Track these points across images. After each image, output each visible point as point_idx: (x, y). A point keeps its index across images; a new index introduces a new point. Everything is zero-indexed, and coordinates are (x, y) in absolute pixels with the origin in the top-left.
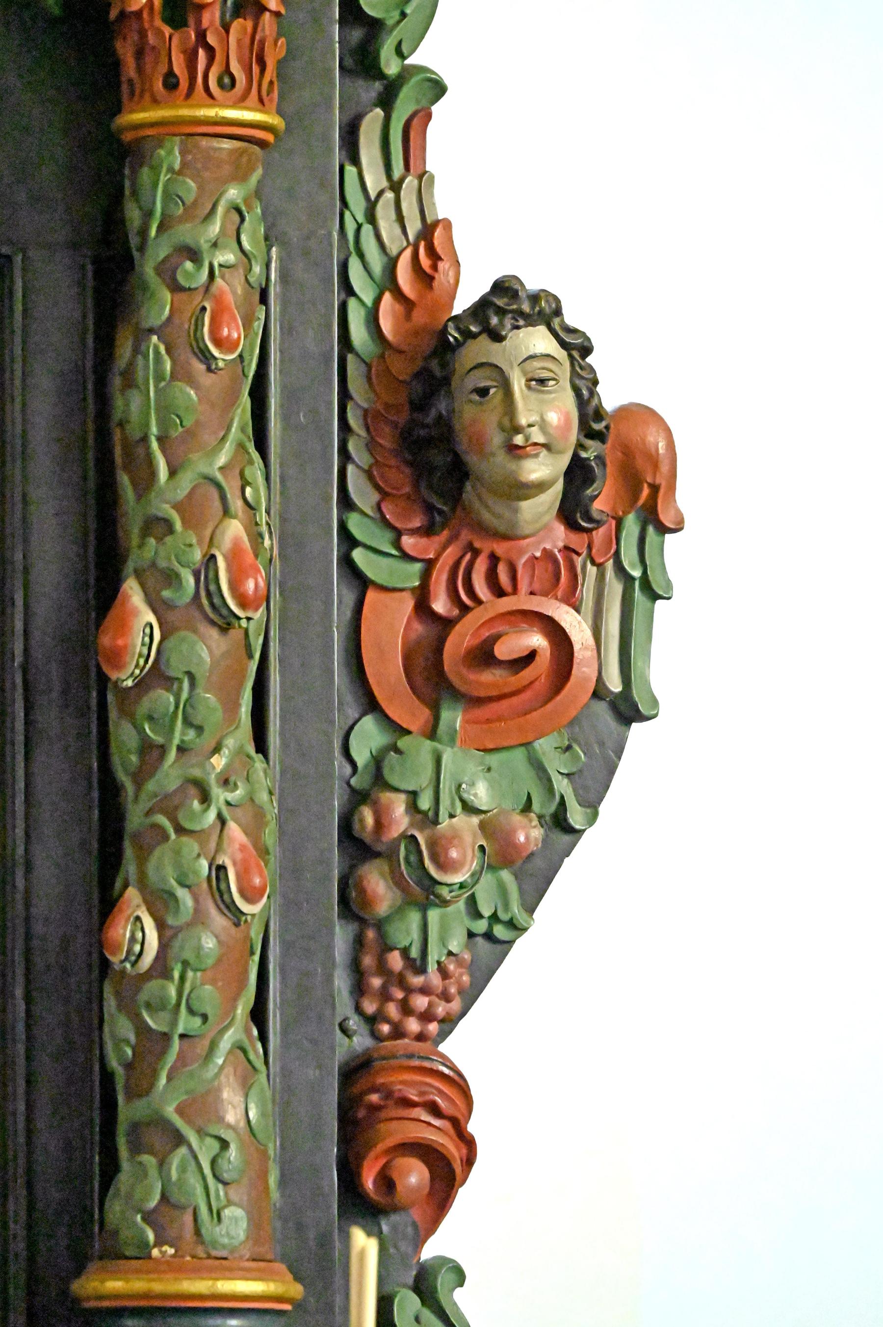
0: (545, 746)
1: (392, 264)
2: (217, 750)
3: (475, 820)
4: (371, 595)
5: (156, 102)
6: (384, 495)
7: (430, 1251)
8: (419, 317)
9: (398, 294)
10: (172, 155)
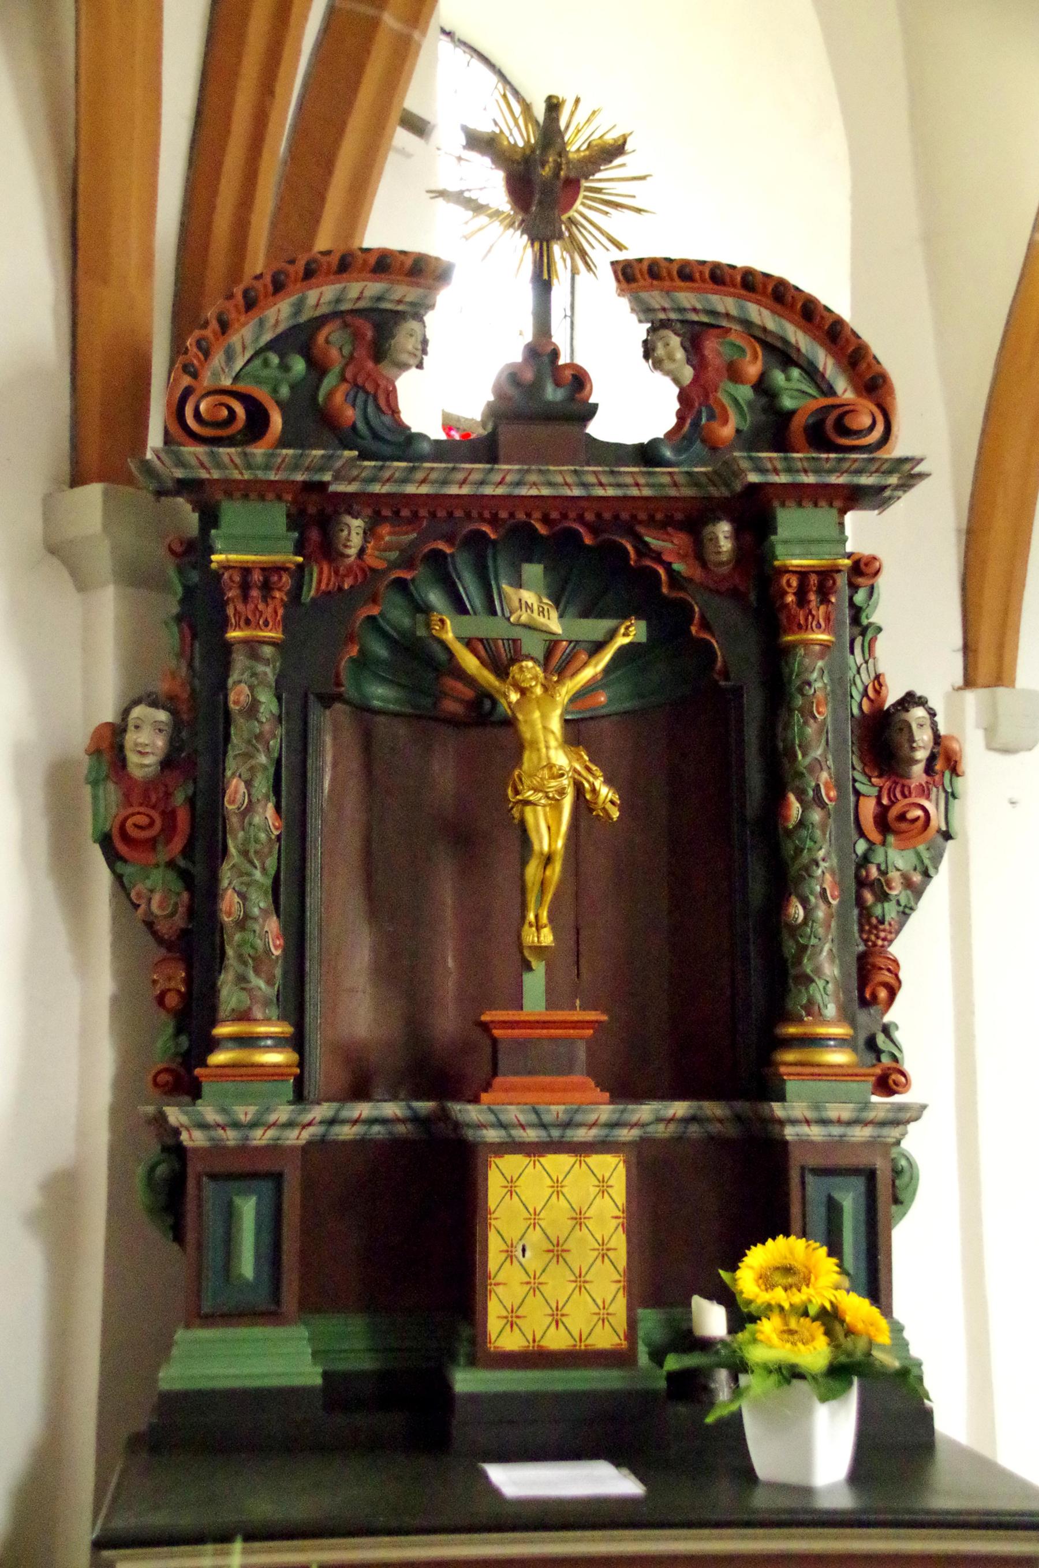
0: (921, 848)
1: (866, 688)
2: (821, 848)
3: (898, 873)
4: (862, 798)
5: (794, 633)
6: (865, 765)
7: (887, 1019)
8: (876, 705)
9: (869, 698)
10: (802, 651)
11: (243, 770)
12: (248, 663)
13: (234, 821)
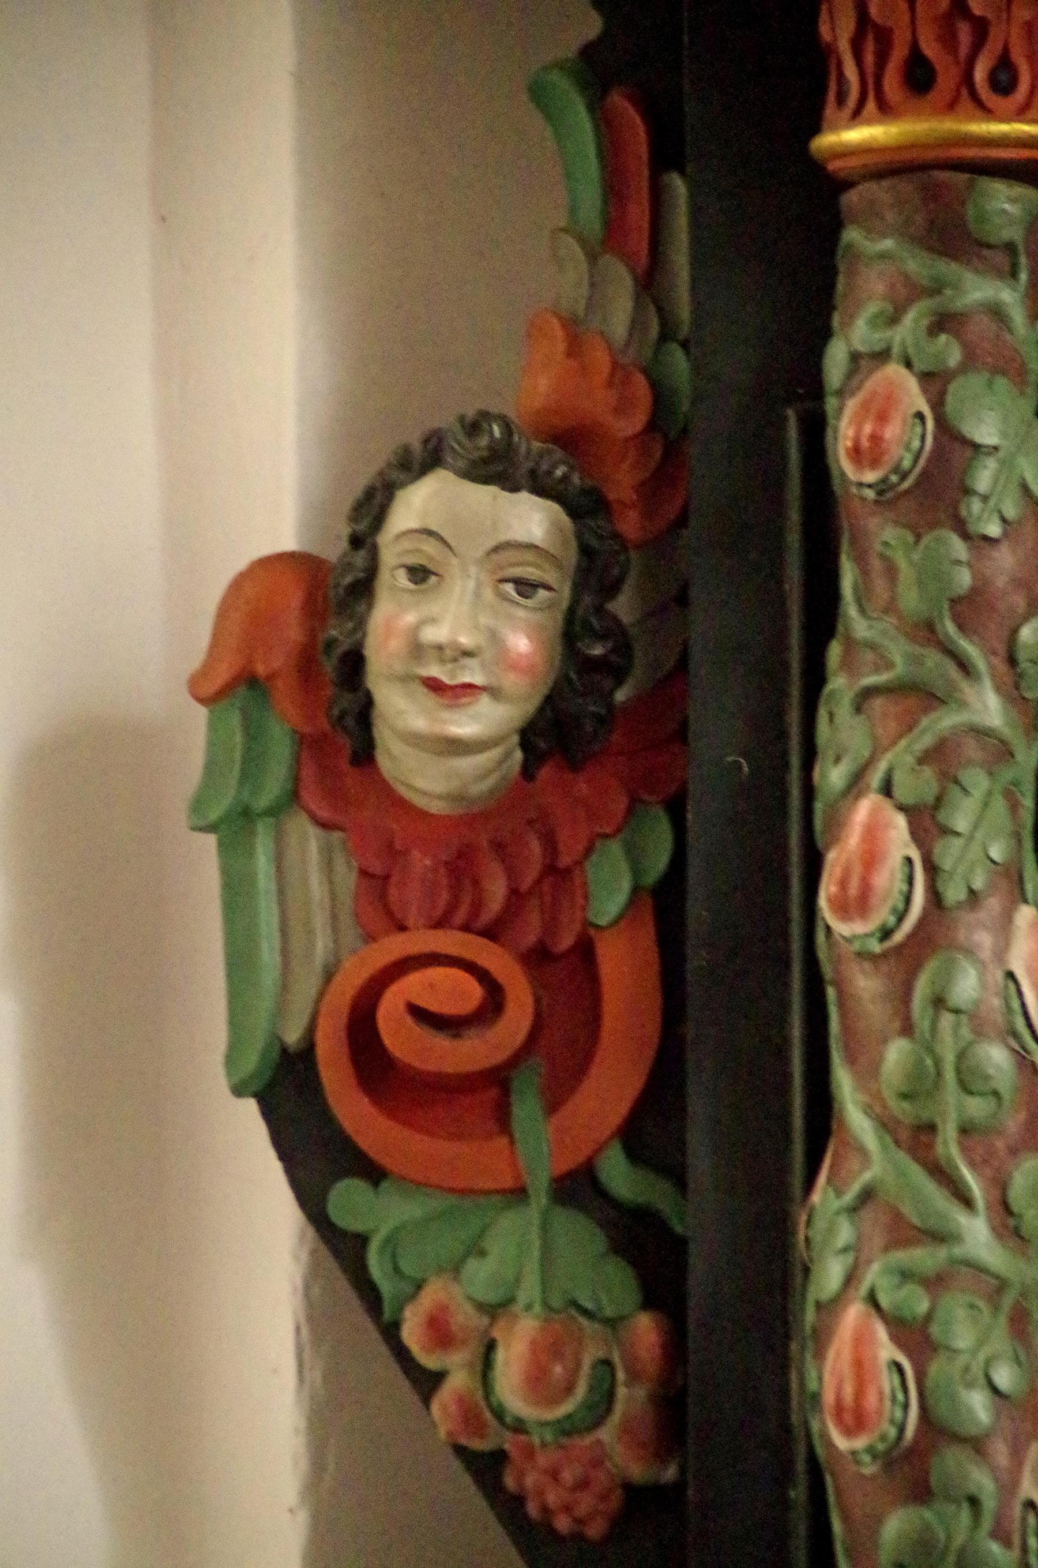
11: (900, 758)
12: (918, 265)
13: (867, 985)
